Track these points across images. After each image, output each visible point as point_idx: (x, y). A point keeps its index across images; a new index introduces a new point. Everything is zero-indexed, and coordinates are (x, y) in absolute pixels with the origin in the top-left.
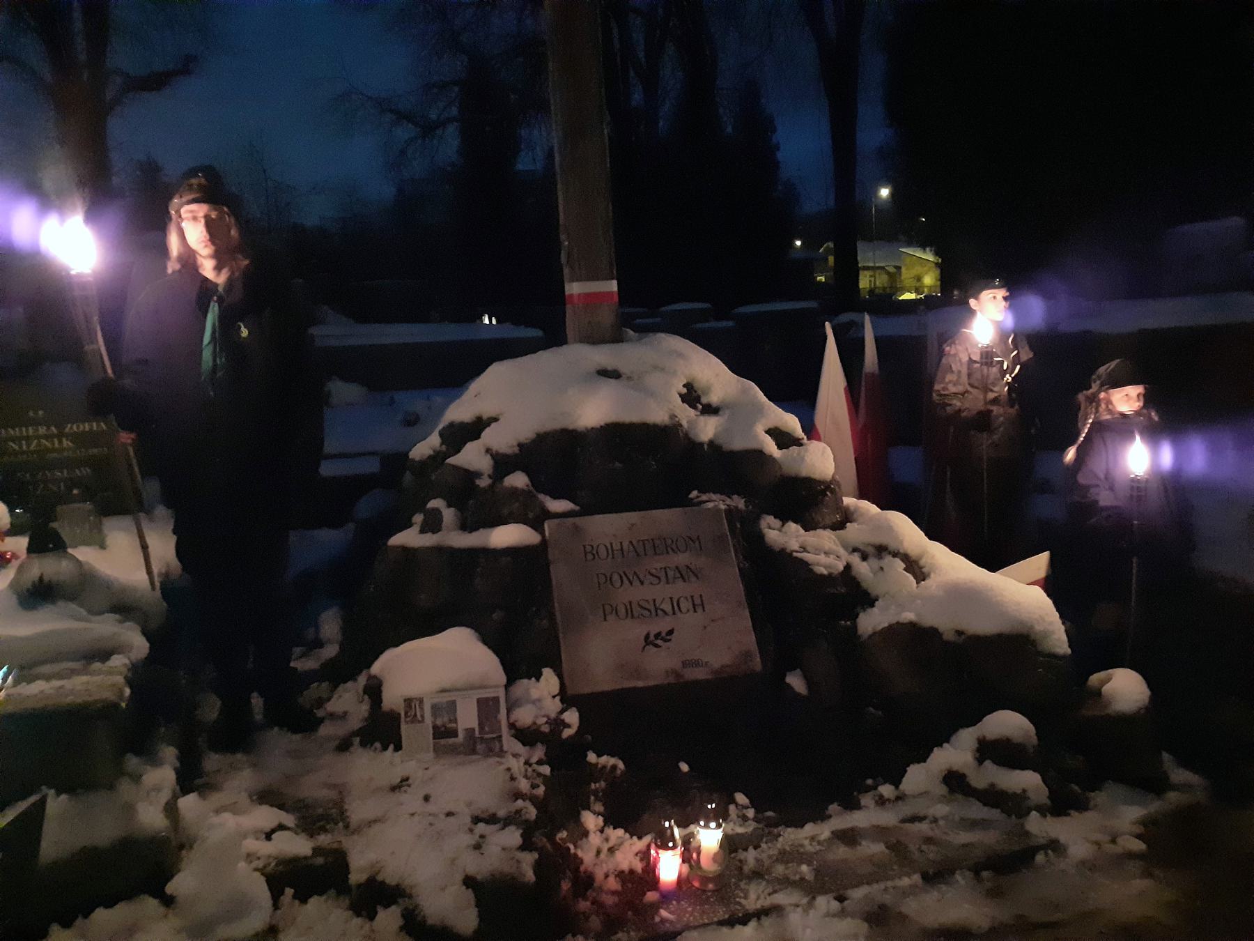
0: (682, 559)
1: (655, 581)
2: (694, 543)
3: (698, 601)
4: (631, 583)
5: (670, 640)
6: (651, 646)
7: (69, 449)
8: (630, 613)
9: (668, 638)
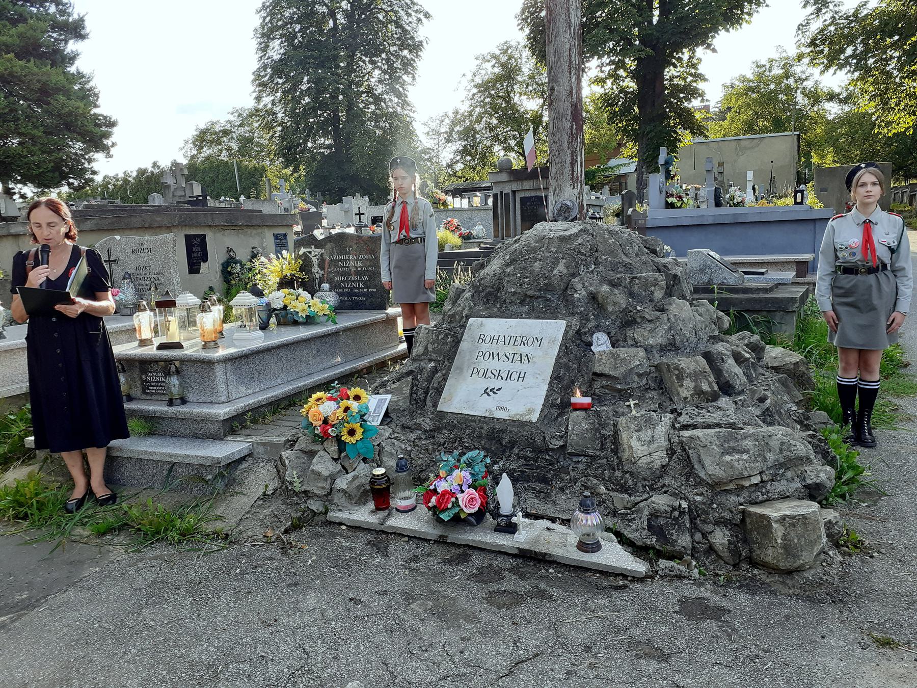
0: (524, 350)
3: (522, 375)
7: (360, 267)
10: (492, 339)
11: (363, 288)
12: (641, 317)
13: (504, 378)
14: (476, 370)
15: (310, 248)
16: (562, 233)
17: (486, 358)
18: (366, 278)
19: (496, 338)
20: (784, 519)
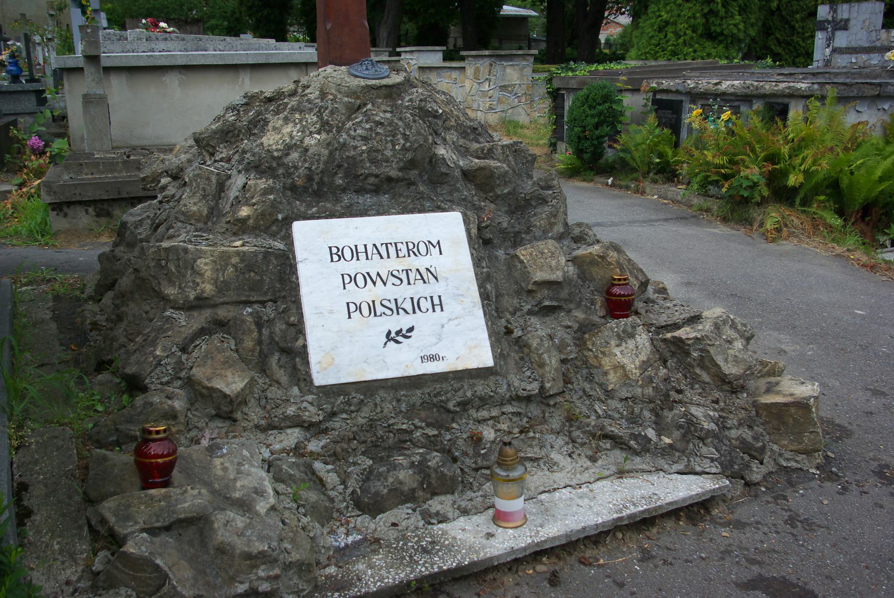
0: (421, 263)
1: (398, 282)
2: (434, 247)
3: (436, 301)
4: (374, 283)
5: (410, 337)
6: (392, 342)
9: (408, 334)
10: (355, 253)
13: (410, 310)
19: (361, 249)
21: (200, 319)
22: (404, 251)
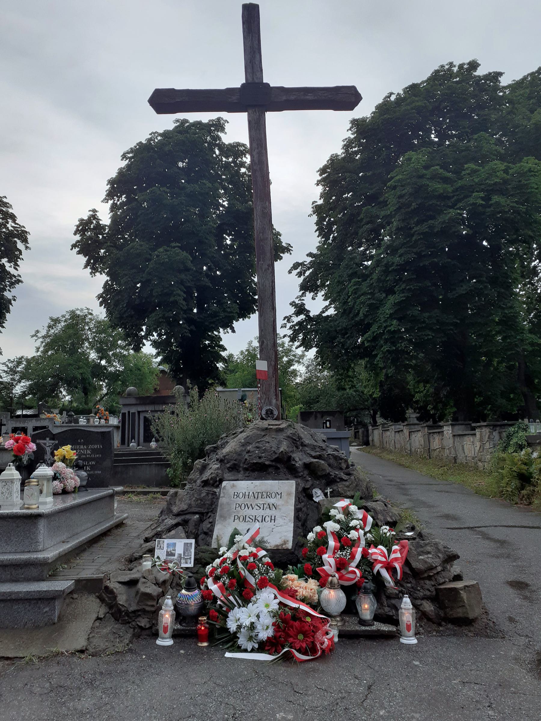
0: (271, 501)
3: (273, 518)
4: (248, 508)
7: (89, 454)
8: (244, 519)
11: (90, 471)
12: (339, 478)
13: (260, 521)
14: (236, 517)
15: (45, 439)
16: (277, 427)
17: (243, 508)
18: (94, 463)
19: (247, 494)
20: (465, 588)
21: (179, 519)
22: (265, 496)
